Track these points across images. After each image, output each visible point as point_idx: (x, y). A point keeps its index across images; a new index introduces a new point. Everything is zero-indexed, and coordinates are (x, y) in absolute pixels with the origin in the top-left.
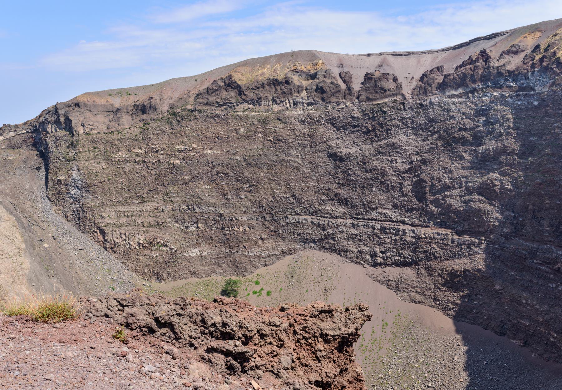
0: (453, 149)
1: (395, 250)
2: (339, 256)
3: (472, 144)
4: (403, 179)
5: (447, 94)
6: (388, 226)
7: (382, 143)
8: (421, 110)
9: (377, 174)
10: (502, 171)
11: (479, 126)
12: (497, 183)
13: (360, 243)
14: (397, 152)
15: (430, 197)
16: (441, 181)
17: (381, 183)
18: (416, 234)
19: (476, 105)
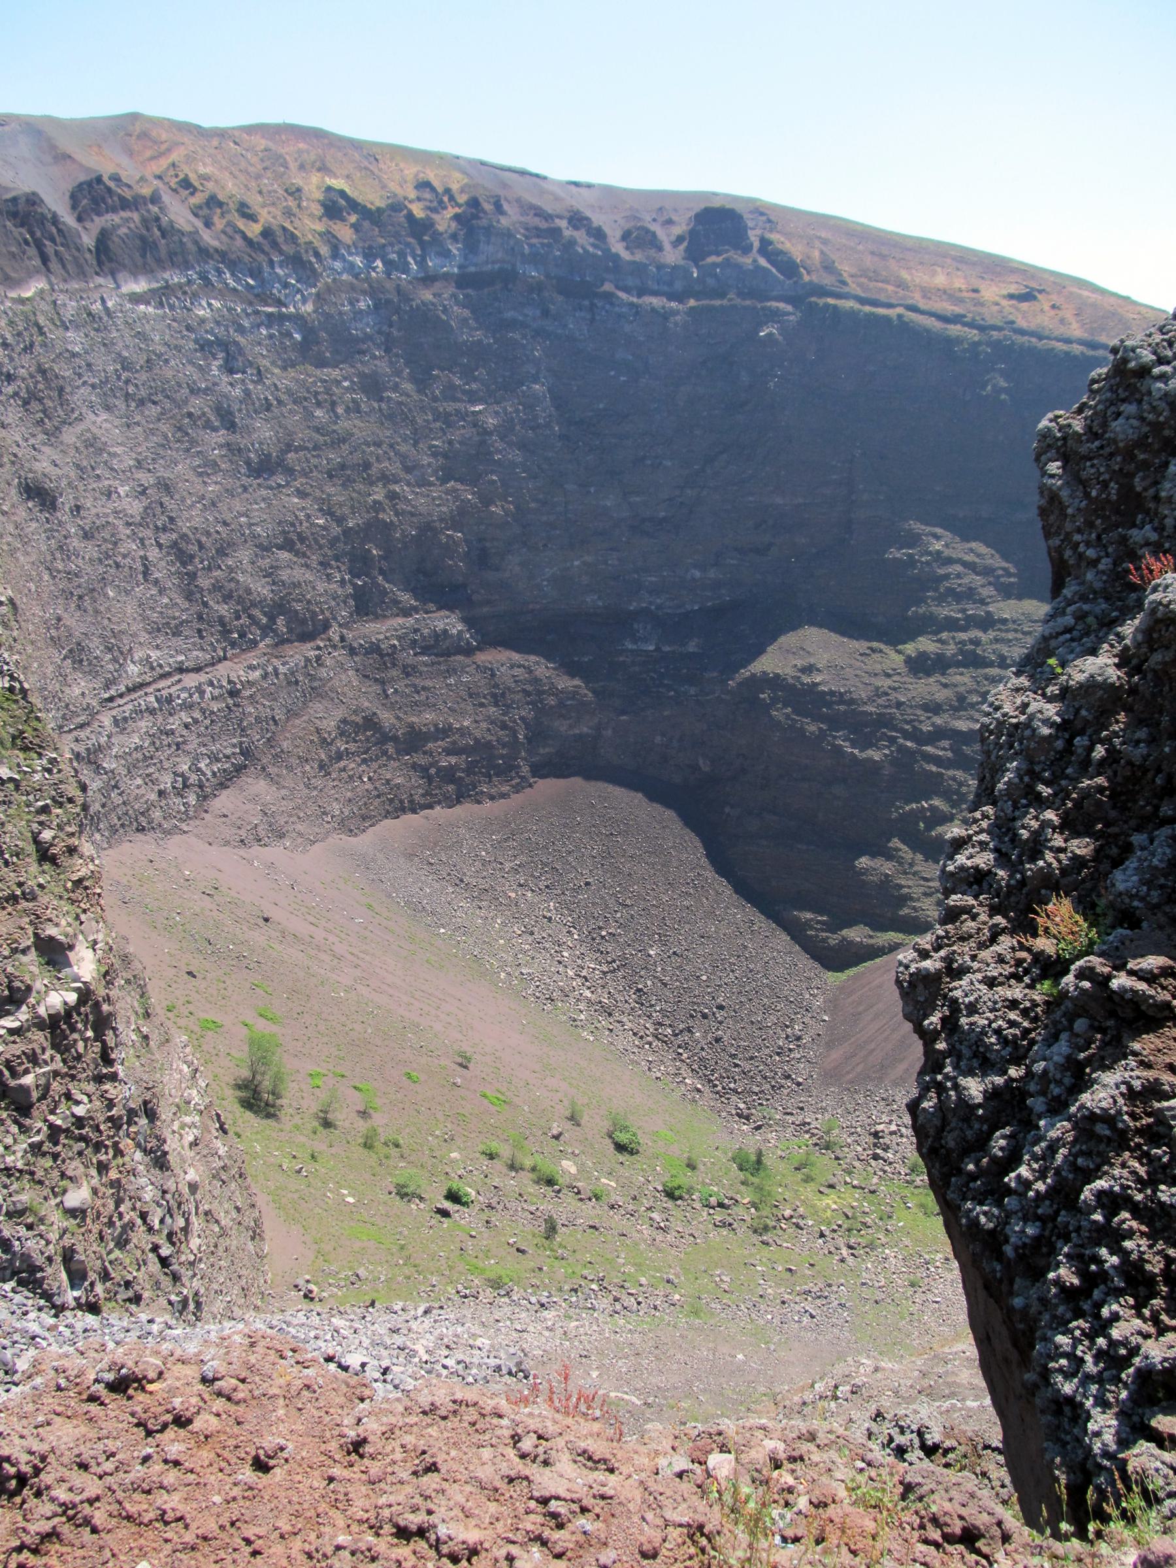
0: (193, 442)
1: (203, 750)
2: (140, 836)
3: (215, 429)
4: (142, 540)
5: (125, 289)
6: (172, 691)
7: (69, 436)
8: (92, 333)
9: (105, 540)
10: (298, 490)
11: (215, 384)
12: (302, 515)
13: (151, 770)
14: (106, 463)
15: (204, 582)
16: (208, 534)
17: (118, 566)
18: (221, 687)
19: (189, 328)
